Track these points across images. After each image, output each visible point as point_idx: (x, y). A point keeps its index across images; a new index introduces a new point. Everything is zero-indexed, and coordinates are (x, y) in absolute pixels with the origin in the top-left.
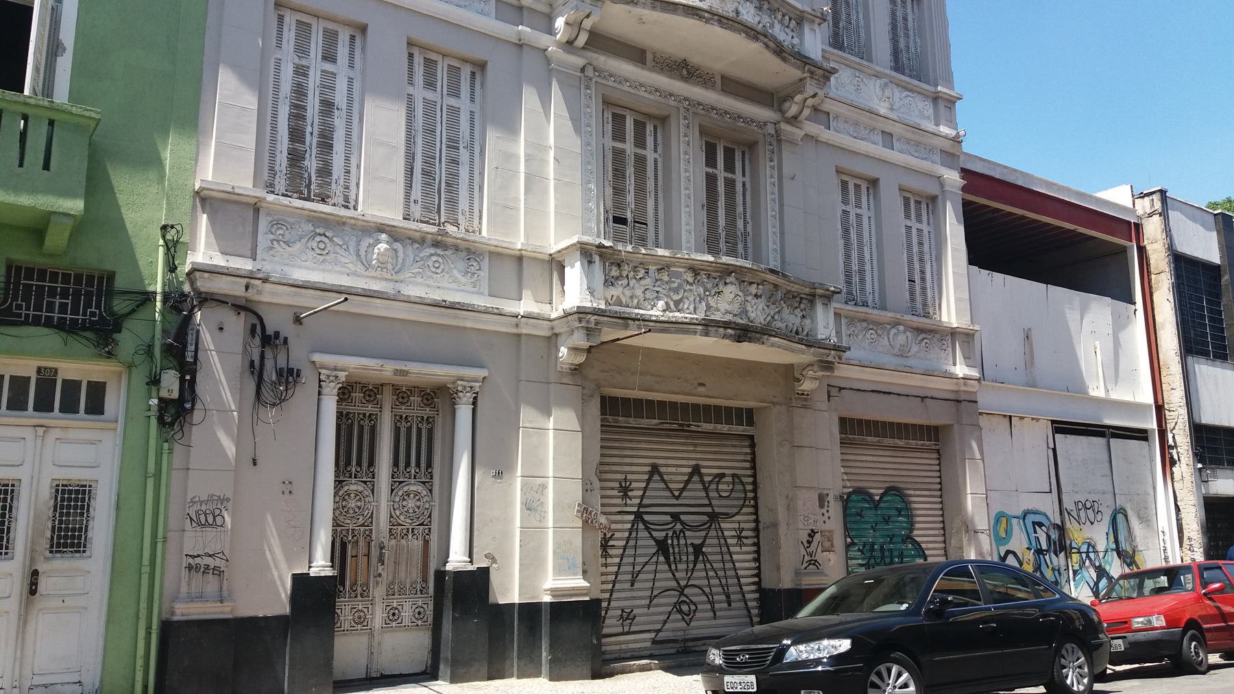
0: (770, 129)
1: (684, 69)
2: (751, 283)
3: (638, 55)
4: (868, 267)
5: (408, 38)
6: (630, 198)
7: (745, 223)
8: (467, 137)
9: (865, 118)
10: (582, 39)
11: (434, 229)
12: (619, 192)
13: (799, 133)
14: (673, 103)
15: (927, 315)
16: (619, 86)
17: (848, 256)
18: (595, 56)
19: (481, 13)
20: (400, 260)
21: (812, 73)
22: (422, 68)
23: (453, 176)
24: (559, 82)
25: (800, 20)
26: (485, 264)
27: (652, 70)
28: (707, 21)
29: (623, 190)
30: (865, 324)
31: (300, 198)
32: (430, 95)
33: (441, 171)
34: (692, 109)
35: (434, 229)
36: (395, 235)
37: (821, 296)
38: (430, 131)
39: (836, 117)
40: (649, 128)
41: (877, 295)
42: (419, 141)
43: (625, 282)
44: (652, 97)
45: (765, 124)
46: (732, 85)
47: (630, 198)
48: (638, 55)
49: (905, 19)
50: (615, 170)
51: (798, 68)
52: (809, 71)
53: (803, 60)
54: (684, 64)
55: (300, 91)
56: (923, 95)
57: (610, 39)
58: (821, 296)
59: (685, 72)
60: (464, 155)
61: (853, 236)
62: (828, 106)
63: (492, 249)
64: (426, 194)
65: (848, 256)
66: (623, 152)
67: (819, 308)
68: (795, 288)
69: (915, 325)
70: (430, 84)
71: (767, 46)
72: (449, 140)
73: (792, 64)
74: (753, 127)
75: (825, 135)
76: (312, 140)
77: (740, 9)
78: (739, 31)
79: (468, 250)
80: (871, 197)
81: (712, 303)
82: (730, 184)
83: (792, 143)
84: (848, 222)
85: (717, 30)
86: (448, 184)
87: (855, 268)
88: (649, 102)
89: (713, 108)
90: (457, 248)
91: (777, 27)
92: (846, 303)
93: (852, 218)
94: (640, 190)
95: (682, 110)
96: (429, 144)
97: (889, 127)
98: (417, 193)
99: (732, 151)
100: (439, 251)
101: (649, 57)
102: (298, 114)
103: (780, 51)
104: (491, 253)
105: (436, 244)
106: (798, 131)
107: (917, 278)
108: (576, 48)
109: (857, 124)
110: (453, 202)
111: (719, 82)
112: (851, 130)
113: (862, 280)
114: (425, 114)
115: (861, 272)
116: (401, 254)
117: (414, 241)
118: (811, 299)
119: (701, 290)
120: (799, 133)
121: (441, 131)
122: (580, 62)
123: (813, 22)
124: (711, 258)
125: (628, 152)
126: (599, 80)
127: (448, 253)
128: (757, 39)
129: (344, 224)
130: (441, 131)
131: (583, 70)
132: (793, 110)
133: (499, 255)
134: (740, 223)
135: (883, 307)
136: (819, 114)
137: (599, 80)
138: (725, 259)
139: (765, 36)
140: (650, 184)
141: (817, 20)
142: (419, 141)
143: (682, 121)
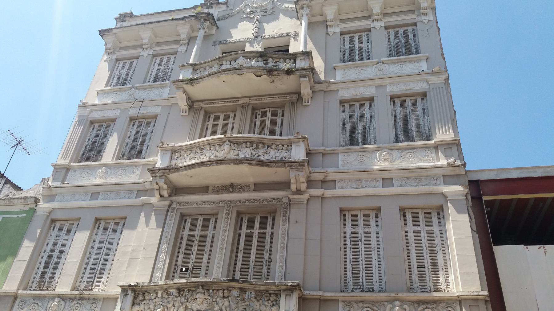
0: (285, 201)
1: (231, 188)
2: (218, 290)
3: (204, 190)
4: (375, 264)
5: (340, 208)
6: (193, 258)
7: (270, 254)
8: (114, 249)
9: (364, 176)
10: (165, 194)
11: (77, 292)
12: (187, 255)
13: (305, 197)
14: (221, 205)
15: (437, 290)
16: (192, 206)
17: (356, 260)
18: (177, 198)
19: (129, 198)
20: (62, 308)
21: (291, 167)
22: (103, 227)
23: (104, 267)
24: (155, 214)
25: (289, 145)
26: (100, 304)
27: (212, 193)
28: (210, 165)
29: (190, 254)
30: (361, 305)
31: (39, 290)
32: (103, 237)
33: (99, 267)
34: (232, 205)
35: (77, 292)
36: (62, 298)
37: (285, 290)
38: (99, 251)
39: (342, 180)
40: (213, 220)
41: (383, 282)
42: (93, 256)
43: (145, 302)
44: (209, 206)
45: (282, 198)
46: (259, 187)
47: (193, 258)
48: (204, 190)
49: (415, 111)
50: (187, 245)
51: (281, 167)
52: (289, 166)
53: (282, 163)
54: (232, 185)
55: (53, 249)
56: (427, 148)
57: (187, 188)
58: (285, 290)
59: (231, 189)
60: (111, 257)
61: (361, 246)
62: (331, 177)
63: (105, 296)
64: (89, 277)
65: (356, 260)
66: (194, 235)
67: (283, 298)
68: (262, 288)
69: (416, 299)
70: (104, 232)
71: (250, 164)
72: (107, 252)
73: (275, 166)
74: (274, 202)
75: (329, 193)
76: (51, 267)
77: (240, 153)
78: (229, 164)
79: (94, 299)
80: (379, 219)
81: (189, 306)
82: (262, 236)
83: (299, 203)
84: (356, 238)
85: (215, 167)
86: (100, 271)
87: (362, 265)
88: (208, 209)
89: (246, 200)
90: (89, 299)
91: (272, 152)
92: (352, 291)
93: (361, 235)
94: (200, 251)
95: (226, 207)
96: (97, 256)
97: (386, 175)
98: (85, 279)
99: (256, 220)
100: (80, 302)
101: (211, 188)
102: (50, 258)
103: (262, 163)
104: (104, 298)
105: (81, 299)
106: (301, 196)
107: (427, 264)
108: (166, 198)
109: (359, 180)
110: (100, 278)
111: (252, 187)
112: (354, 185)
113: (369, 274)
114: (99, 244)
115: (369, 269)
116: (63, 306)
117: (70, 299)
118: (277, 293)
119: (183, 299)
120: (305, 197)
121: (104, 250)
122: (167, 203)
123: (299, 141)
124: (184, 281)
125: (196, 235)
126: (179, 207)
127: (84, 302)
128: (242, 163)
129: (46, 297)
130: (104, 250)
131: (170, 206)
132: (293, 187)
133: (108, 298)
134: (266, 256)
135: (382, 291)
136: (324, 183)
137: (179, 207)
138: (193, 280)
139: (247, 160)
140: (207, 247)
141: (301, 140)
142: (93, 256)
143: (225, 212)
